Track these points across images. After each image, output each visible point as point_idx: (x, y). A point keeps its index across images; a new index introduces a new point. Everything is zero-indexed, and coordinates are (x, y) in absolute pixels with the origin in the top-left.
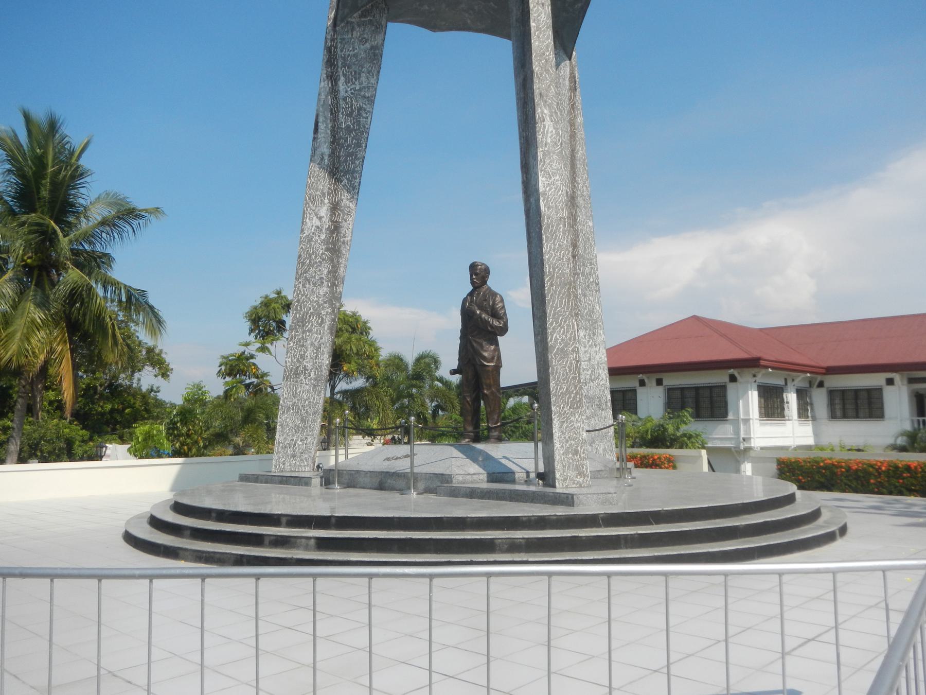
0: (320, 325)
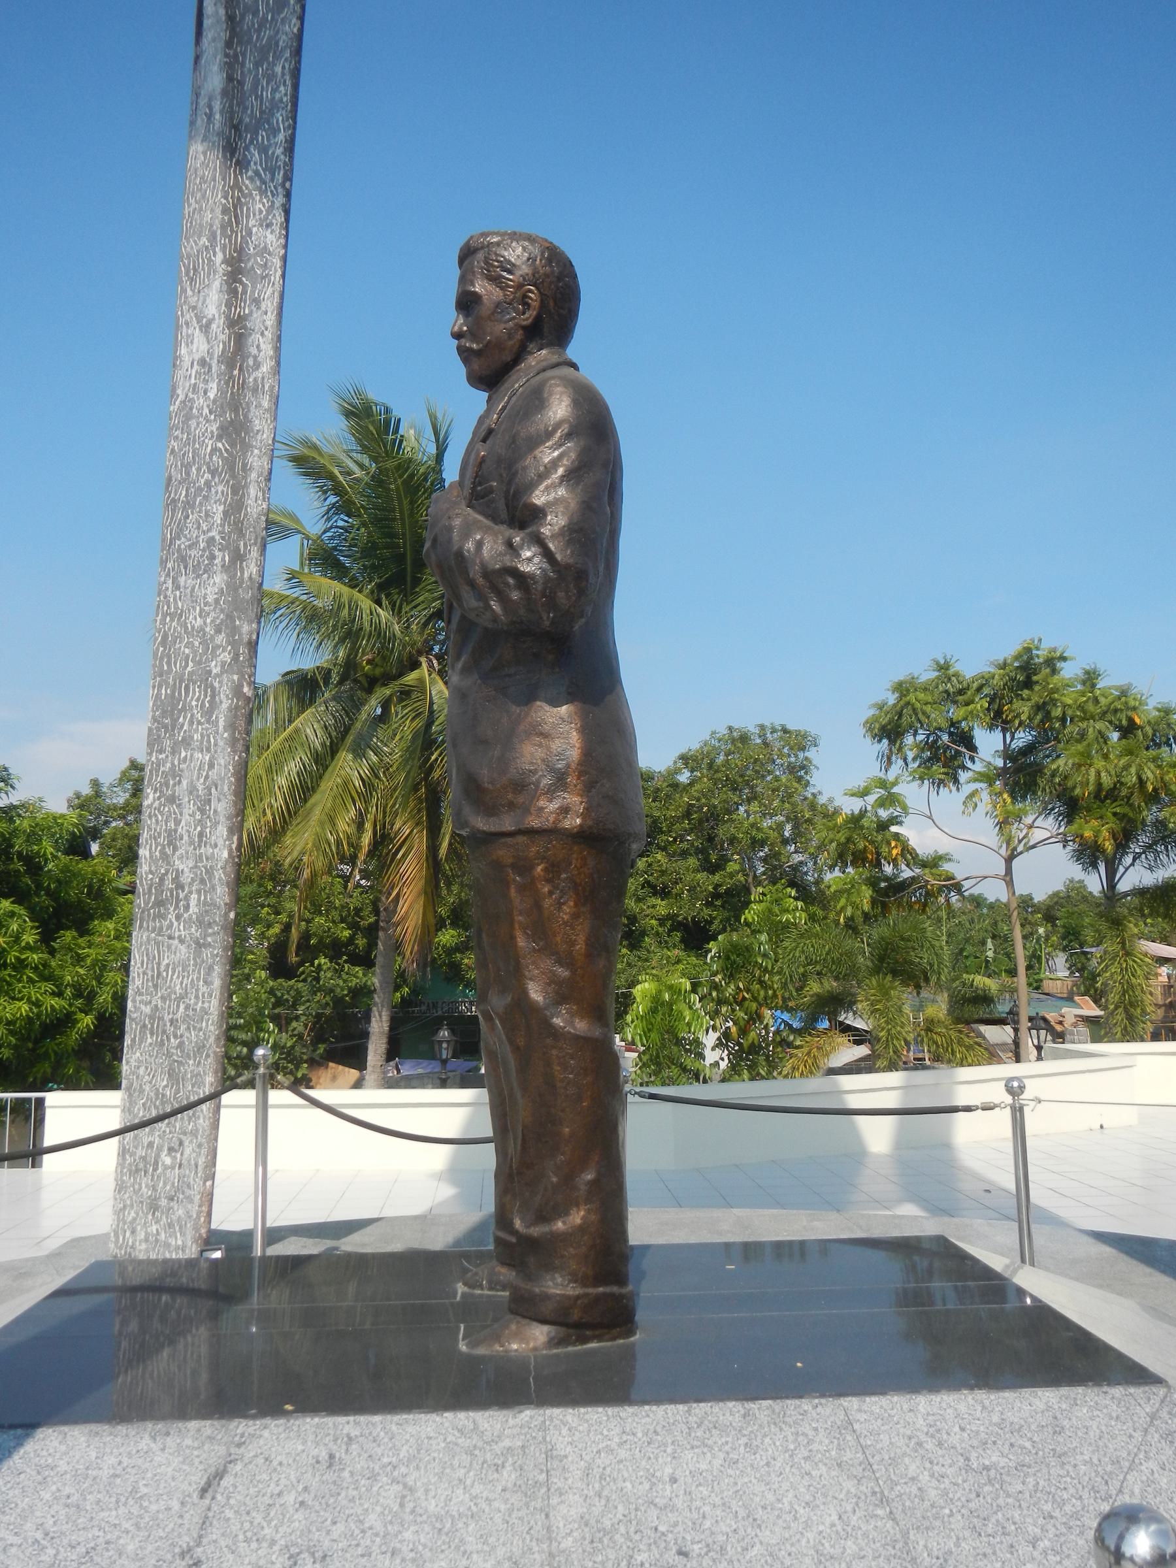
0: (209, 713)
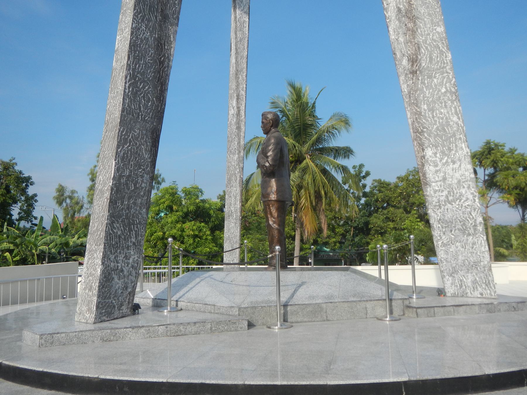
0: (236, 181)
